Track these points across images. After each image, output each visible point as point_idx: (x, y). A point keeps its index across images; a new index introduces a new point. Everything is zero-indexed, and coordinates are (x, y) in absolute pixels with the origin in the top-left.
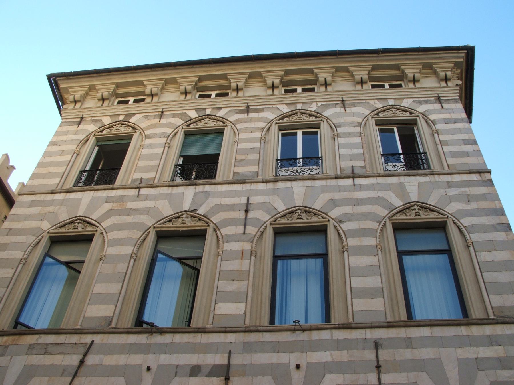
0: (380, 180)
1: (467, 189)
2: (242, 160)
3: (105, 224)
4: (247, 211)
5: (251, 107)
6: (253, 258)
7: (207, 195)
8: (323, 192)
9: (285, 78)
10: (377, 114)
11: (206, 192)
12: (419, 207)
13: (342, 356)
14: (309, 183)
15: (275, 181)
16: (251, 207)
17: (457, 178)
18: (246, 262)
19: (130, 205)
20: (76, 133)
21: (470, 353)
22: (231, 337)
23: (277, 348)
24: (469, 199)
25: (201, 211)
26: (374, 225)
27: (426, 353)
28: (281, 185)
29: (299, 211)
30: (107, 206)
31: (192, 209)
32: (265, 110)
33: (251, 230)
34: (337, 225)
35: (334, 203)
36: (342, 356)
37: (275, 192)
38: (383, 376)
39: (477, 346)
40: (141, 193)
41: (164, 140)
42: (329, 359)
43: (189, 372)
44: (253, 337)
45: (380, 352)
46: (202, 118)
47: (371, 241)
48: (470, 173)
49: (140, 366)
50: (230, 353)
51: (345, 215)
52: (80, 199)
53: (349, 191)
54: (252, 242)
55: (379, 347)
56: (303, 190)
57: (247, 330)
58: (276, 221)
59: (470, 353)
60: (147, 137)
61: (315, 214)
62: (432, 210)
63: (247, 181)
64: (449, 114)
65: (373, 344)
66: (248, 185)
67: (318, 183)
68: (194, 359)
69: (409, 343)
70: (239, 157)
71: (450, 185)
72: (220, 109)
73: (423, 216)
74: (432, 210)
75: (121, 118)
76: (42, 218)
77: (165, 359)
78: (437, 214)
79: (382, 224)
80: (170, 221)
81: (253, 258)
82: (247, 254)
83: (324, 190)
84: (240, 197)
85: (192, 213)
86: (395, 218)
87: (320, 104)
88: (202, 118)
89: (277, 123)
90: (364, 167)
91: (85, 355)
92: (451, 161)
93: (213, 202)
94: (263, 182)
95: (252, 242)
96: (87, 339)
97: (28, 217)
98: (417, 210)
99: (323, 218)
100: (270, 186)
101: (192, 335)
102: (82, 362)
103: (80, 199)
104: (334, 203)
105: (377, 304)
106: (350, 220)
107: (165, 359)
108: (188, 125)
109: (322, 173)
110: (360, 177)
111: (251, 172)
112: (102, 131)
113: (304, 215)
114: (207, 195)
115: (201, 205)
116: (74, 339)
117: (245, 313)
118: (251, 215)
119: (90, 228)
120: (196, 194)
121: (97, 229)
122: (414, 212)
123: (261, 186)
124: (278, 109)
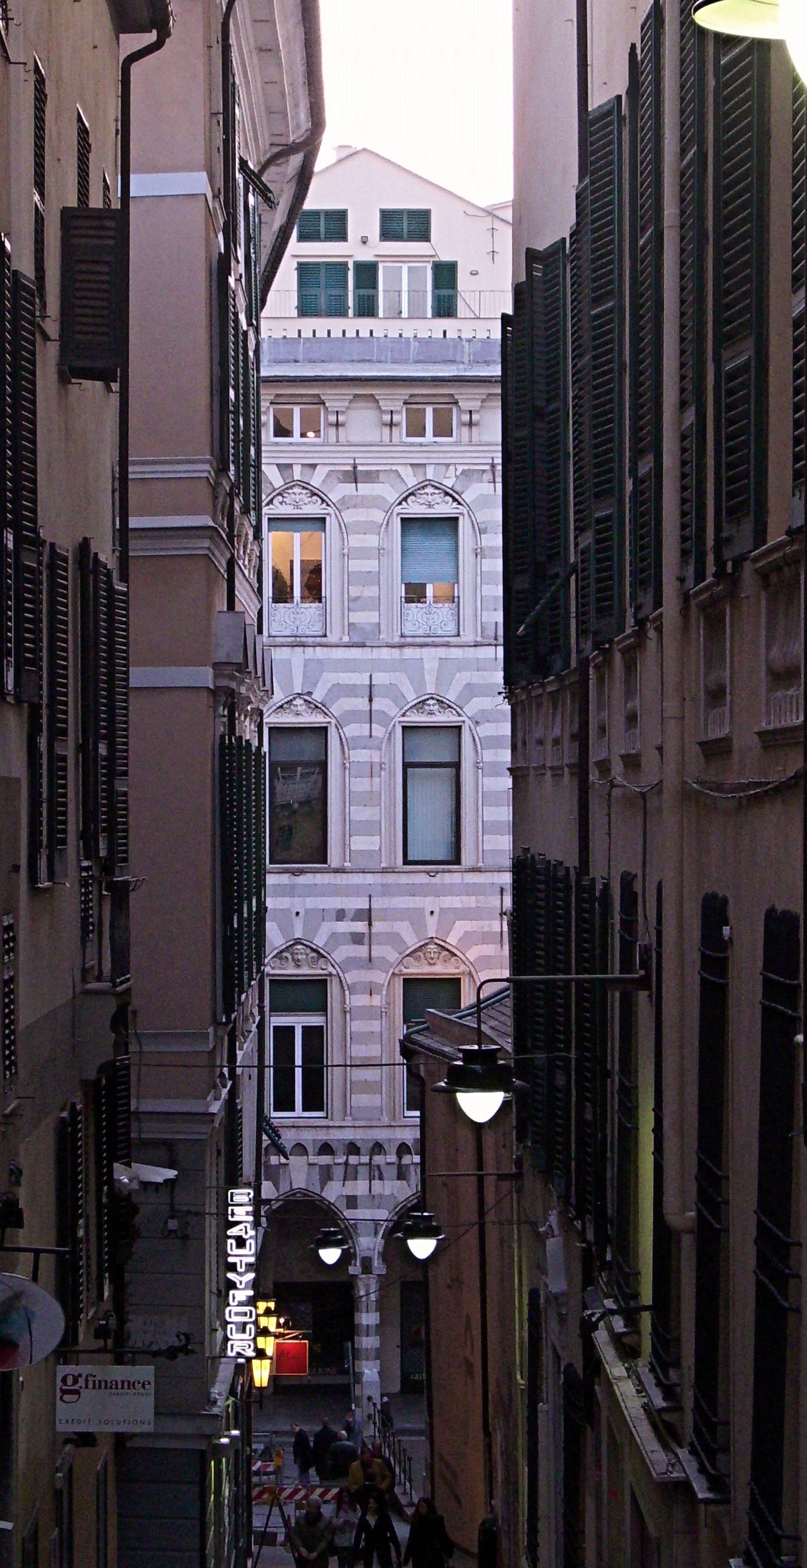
2: (358, 598)
4: (371, 700)
7: (319, 661)
8: (459, 670)
11: (319, 661)
13: (471, 901)
14: (442, 652)
15: (401, 646)
16: (375, 690)
18: (376, 780)
22: (370, 878)
23: (413, 891)
25: (318, 696)
28: (409, 652)
29: (431, 702)
31: (306, 691)
32: (381, 475)
34: (473, 727)
36: (471, 901)
37: (401, 666)
42: (459, 905)
44: (390, 879)
49: (289, 910)
50: (370, 896)
51: (482, 711)
53: (490, 670)
54: (380, 749)
56: (435, 664)
57: (384, 871)
61: (450, 707)
66: (369, 649)
68: (337, 903)
70: (354, 591)
77: (312, 903)
80: (281, 707)
81: (383, 773)
83: (462, 665)
84: (360, 671)
85: (306, 696)
87: (460, 469)
89: (398, 514)
93: (329, 679)
95: (380, 749)
100: (396, 652)
101: (332, 875)
106: (488, 721)
107: (312, 903)
109: (458, 635)
111: (370, 624)
115: (315, 684)
118: (376, 706)
120: (307, 663)
123: (385, 653)
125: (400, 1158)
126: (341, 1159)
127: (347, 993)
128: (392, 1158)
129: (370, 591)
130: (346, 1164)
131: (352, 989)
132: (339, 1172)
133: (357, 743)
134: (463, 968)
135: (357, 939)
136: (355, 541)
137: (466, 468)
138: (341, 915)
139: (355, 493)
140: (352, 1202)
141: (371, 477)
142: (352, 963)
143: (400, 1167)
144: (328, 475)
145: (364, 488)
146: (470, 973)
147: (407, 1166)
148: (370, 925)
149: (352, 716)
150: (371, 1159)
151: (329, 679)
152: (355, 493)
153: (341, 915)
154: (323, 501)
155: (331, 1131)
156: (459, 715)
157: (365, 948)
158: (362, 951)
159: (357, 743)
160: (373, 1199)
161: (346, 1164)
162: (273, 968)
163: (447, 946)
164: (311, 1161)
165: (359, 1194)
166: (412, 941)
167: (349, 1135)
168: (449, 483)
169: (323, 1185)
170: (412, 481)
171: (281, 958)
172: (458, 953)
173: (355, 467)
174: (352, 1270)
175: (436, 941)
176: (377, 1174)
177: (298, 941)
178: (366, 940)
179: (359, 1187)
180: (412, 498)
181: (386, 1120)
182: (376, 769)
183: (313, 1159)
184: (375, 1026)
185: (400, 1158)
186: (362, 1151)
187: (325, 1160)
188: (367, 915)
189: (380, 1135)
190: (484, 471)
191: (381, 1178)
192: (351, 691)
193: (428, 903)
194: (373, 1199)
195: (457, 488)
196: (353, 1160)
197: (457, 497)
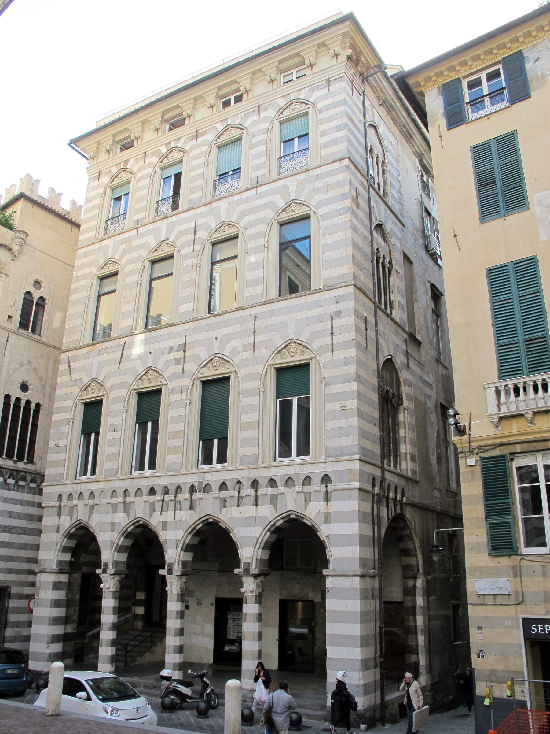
0: (273, 185)
1: (328, 179)
2: (193, 188)
3: (123, 262)
4: (195, 233)
5: (199, 132)
6: (198, 268)
7: (174, 224)
9: (220, 93)
10: (282, 113)
12: (295, 205)
13: (237, 328)
14: (230, 199)
17: (324, 169)
19: (134, 243)
20: (98, 187)
21: (302, 315)
24: (328, 188)
26: (264, 227)
27: (280, 319)
30: (123, 247)
32: (208, 132)
33: (198, 247)
35: (244, 214)
36: (237, 328)
38: (256, 337)
39: (308, 309)
40: (139, 232)
41: (147, 181)
42: (231, 331)
43: (168, 351)
45: (256, 322)
46: (170, 152)
47: (261, 241)
48: (334, 162)
52: (108, 245)
55: (257, 319)
58: (211, 237)
59: (302, 315)
60: (139, 180)
61: (233, 225)
62: (304, 205)
63: (195, 207)
64: (332, 98)
65: (253, 318)
66: (196, 210)
67: (237, 197)
69: (272, 313)
71: (318, 177)
72: (180, 139)
73: (297, 212)
74: (304, 205)
75: (122, 166)
76: (91, 264)
78: (305, 207)
79: (270, 225)
80: (156, 250)
81: (198, 268)
82: (195, 267)
86: (279, 217)
87: (243, 114)
88: (170, 152)
90: (265, 175)
91: (123, 351)
92: (324, 152)
93: (178, 229)
94: (204, 205)
96: (122, 341)
97: (85, 266)
98: (293, 208)
99: (237, 228)
100: (208, 207)
102: (122, 355)
103: (108, 245)
104: (244, 214)
105: (259, 289)
108: (162, 162)
110: (260, 186)
112: (113, 181)
113: (226, 228)
114: (174, 224)
116: (116, 342)
117: (193, 309)
119: (116, 267)
121: (120, 266)
122: (291, 209)
123: (203, 209)
124: (216, 128)
125: (191, 495)
126: (160, 498)
127: (170, 394)
128: (187, 495)
129: (199, 183)
130: (163, 501)
131: (173, 391)
132: (158, 506)
133: (187, 257)
134: (232, 369)
135: (177, 361)
136: (194, 163)
137: (246, 112)
138: (171, 350)
139: (196, 143)
140: (165, 526)
141: (204, 134)
142: (175, 376)
143: (191, 500)
144: (186, 140)
145: (200, 140)
146: (236, 371)
147: (195, 500)
148: (185, 352)
149: (185, 245)
150: (175, 497)
151: (178, 229)
152: (196, 143)
153: (171, 350)
154: (184, 152)
155: (156, 479)
156: (237, 228)
157: (182, 365)
158: (179, 368)
159: (187, 257)
160: (176, 524)
161: (163, 501)
162: (138, 386)
163: (224, 357)
164: (145, 499)
165: (168, 520)
166: (205, 356)
167: (164, 481)
168: (237, 122)
169: (151, 515)
170: (220, 127)
171: (142, 381)
172: (230, 360)
173: (197, 132)
174: (162, 572)
175: (218, 355)
176: (179, 506)
177: (149, 369)
178: (182, 362)
179: (168, 516)
180: (222, 136)
181: (183, 471)
182: (195, 267)
183: (146, 498)
184: (182, 411)
185: (191, 495)
186: (170, 492)
187: (152, 498)
188: (184, 348)
189: (180, 480)
190: (254, 111)
191: (180, 510)
192: (186, 232)
193: (214, 334)
194: (176, 524)
195: (241, 123)
196: (167, 498)
197: (242, 127)
